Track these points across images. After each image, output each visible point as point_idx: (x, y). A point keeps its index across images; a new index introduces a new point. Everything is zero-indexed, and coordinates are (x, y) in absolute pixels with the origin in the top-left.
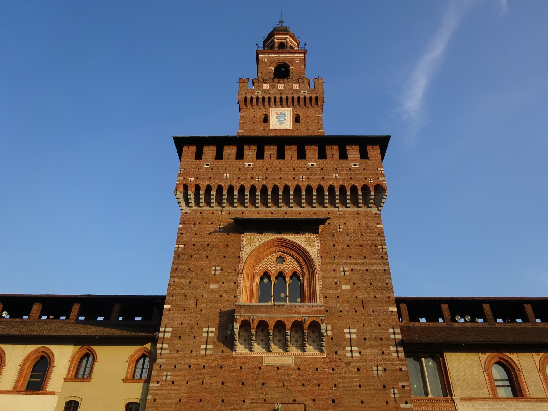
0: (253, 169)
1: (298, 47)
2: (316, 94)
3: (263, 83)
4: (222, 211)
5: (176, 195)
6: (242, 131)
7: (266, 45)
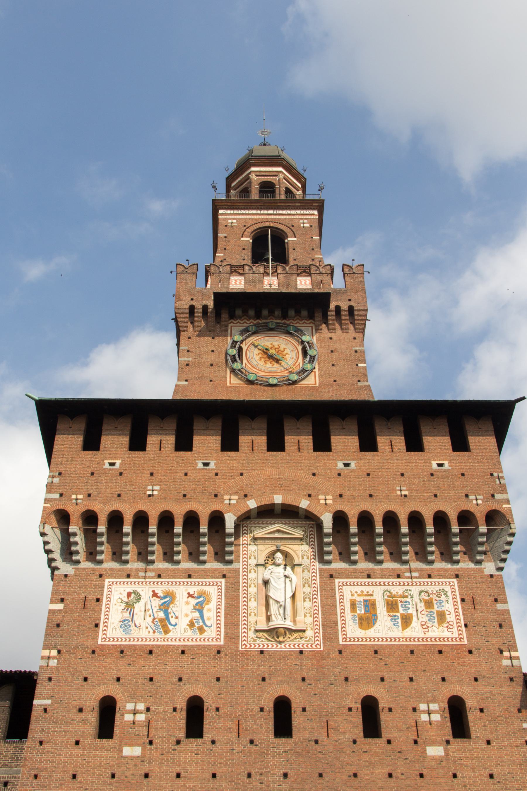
0: (217, 474)
1: (304, 192)
2: (350, 300)
3: (231, 273)
4: (146, 572)
5: (43, 534)
6: (186, 383)
7: (233, 185)
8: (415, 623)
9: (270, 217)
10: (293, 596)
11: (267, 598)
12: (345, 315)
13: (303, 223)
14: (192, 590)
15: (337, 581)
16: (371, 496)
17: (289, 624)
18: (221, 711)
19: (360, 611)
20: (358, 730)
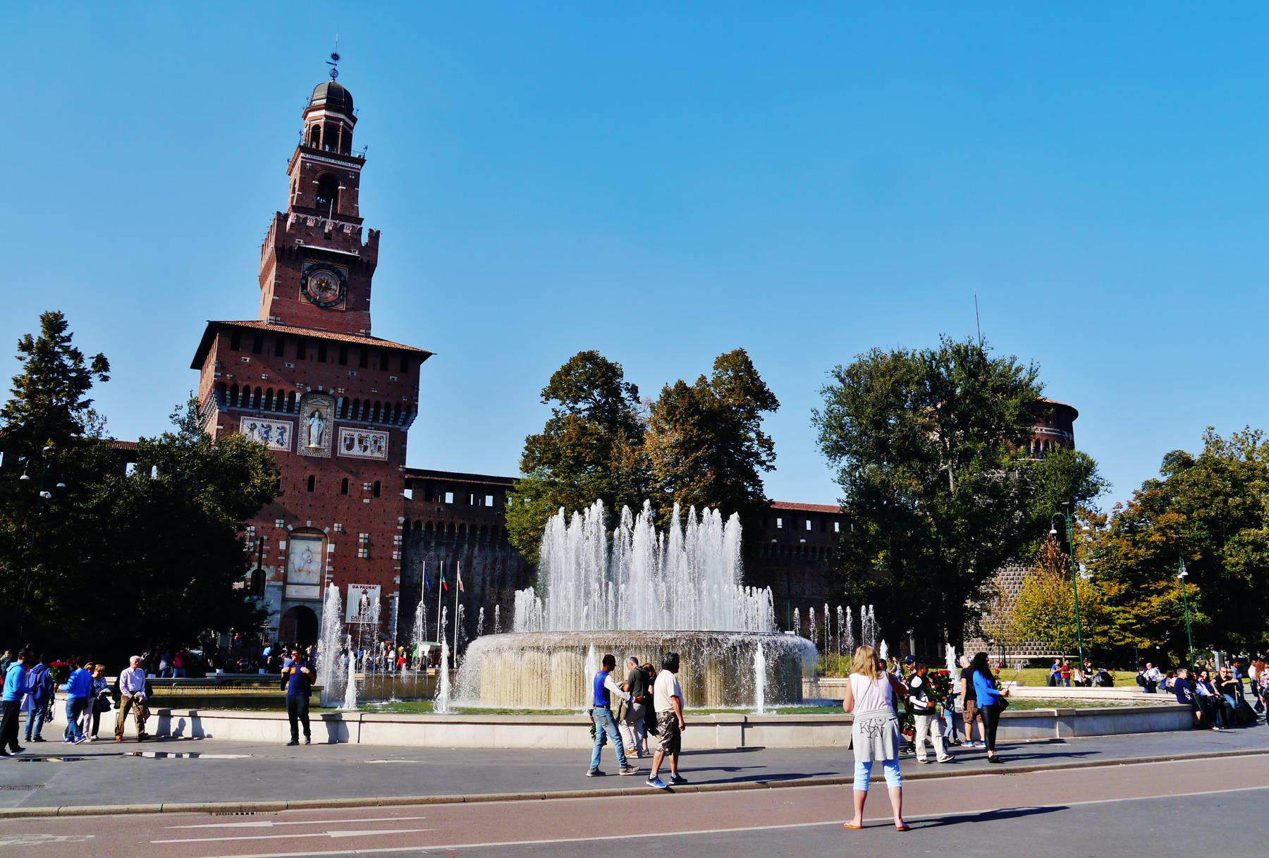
2: (369, 256)
6: (277, 298)
7: (311, 115)
8: (369, 450)
9: (333, 166)
13: (352, 175)
14: (279, 425)
16: (361, 391)
18: (289, 479)
19: (348, 442)
20: (339, 490)
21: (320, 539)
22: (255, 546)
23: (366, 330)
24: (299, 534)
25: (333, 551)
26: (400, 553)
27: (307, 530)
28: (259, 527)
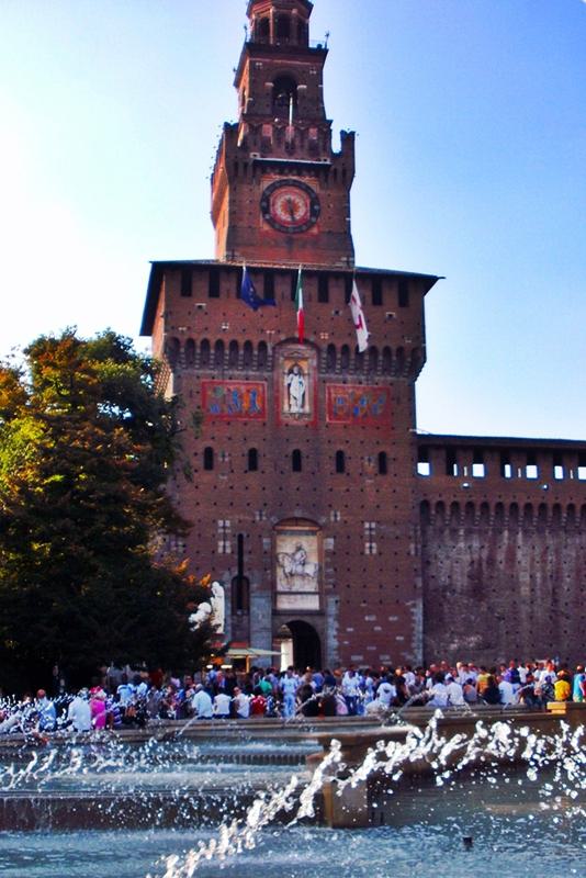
10: (304, 395)
11: (289, 394)
12: (339, 175)
15: (328, 384)
17: (301, 411)
20: (334, 468)
21: (313, 533)
22: (231, 546)
23: (348, 257)
24: (288, 528)
25: (331, 547)
26: (419, 546)
27: (296, 521)
28: (237, 521)
